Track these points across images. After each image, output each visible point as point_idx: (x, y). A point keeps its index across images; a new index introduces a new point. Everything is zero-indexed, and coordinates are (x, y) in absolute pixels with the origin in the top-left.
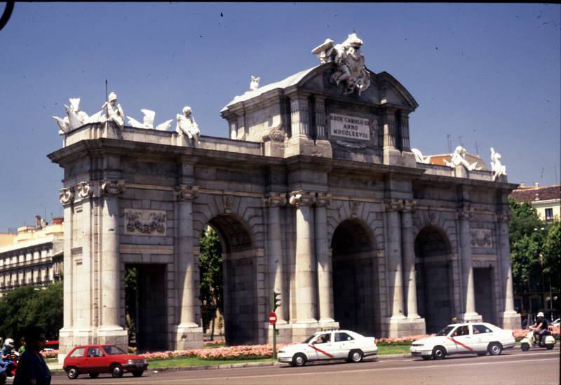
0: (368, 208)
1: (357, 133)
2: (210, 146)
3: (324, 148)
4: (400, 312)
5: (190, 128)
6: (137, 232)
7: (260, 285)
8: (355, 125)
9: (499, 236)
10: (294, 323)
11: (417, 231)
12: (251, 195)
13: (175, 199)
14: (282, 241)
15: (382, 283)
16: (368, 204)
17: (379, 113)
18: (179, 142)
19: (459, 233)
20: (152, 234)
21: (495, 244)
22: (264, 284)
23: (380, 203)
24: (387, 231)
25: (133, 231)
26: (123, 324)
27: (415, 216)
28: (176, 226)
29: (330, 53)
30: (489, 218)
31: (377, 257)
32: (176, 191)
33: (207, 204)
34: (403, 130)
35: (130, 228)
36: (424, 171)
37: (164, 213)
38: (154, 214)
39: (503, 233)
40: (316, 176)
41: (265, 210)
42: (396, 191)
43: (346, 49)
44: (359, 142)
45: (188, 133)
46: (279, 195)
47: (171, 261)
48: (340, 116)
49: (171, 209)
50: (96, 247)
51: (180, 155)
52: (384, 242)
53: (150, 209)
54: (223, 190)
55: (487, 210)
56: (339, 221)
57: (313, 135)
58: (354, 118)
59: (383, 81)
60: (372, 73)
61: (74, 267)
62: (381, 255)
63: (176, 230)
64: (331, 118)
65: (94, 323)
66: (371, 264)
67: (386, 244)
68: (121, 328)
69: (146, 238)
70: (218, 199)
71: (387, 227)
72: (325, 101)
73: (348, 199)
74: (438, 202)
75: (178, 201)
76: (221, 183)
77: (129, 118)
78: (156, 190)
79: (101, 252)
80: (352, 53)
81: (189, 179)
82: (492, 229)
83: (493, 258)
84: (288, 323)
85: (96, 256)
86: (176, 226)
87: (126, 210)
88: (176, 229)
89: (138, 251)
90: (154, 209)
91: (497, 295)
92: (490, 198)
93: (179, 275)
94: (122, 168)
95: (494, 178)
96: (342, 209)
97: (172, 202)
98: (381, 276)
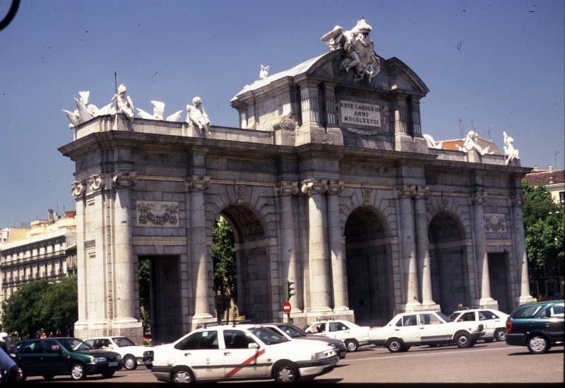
0: (381, 194)
1: (368, 120)
2: (220, 136)
3: (335, 136)
4: (415, 298)
5: (200, 117)
6: (149, 224)
7: (274, 274)
8: (365, 111)
9: (514, 220)
10: (308, 311)
11: (431, 218)
12: (263, 184)
13: (187, 190)
14: (295, 230)
15: (396, 270)
16: (379, 192)
17: (389, 99)
18: (190, 133)
19: (472, 218)
21: (509, 229)
22: (278, 274)
23: (392, 190)
24: (401, 218)
25: (145, 223)
26: (137, 316)
27: (428, 201)
28: (188, 217)
29: (339, 39)
30: (503, 202)
31: (390, 245)
32: (188, 182)
34: (414, 115)
36: (437, 156)
37: (176, 204)
38: (166, 206)
39: (517, 217)
40: (328, 163)
41: (277, 199)
42: (408, 177)
43: (355, 36)
44: (370, 129)
45: (198, 124)
46: (291, 184)
47: (183, 252)
48: (350, 103)
49: (183, 200)
50: (109, 239)
51: (191, 145)
52: (397, 229)
53: (162, 201)
54: (234, 181)
55: (500, 194)
56: (352, 208)
57: (323, 123)
58: (364, 105)
59: (393, 67)
61: (88, 260)
62: (394, 241)
63: (188, 221)
64: (342, 105)
65: (108, 315)
66: (385, 251)
67: (399, 231)
68: (136, 320)
70: (230, 189)
71: (400, 214)
72: (336, 88)
73: (359, 186)
74: (451, 187)
75: (190, 192)
76: (231, 172)
77: (139, 109)
78: (167, 181)
79: (114, 245)
80: (361, 40)
81: (199, 170)
82: (506, 214)
83: (508, 243)
84: (303, 312)
85: (109, 249)
86: (188, 217)
87: (138, 202)
88: (188, 220)
89: (151, 243)
90: (167, 201)
91: (512, 280)
92: (503, 182)
93: (192, 266)
94: (133, 160)
95: (507, 162)
96: (354, 198)
97: (184, 193)
98: (395, 263)
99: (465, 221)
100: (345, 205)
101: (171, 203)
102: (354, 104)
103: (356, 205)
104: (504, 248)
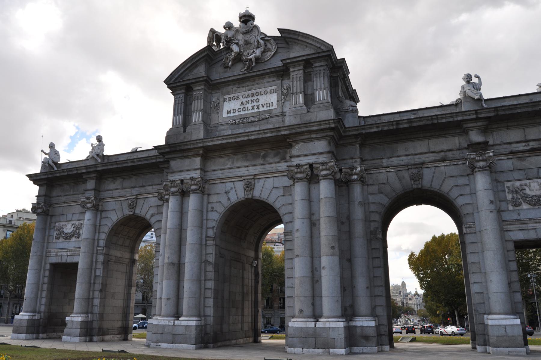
0: (270, 183)
6: (61, 240)
8: (256, 98)
19: (473, 193)
20: (71, 240)
35: (57, 238)
37: (81, 222)
40: (187, 162)
44: (260, 113)
48: (236, 95)
53: (72, 220)
54: (125, 196)
56: (227, 204)
58: (254, 91)
60: (274, 38)
64: (225, 100)
87: (57, 224)
99: (461, 197)
100: (220, 202)
101: (78, 221)
102: (241, 95)
103: (234, 199)
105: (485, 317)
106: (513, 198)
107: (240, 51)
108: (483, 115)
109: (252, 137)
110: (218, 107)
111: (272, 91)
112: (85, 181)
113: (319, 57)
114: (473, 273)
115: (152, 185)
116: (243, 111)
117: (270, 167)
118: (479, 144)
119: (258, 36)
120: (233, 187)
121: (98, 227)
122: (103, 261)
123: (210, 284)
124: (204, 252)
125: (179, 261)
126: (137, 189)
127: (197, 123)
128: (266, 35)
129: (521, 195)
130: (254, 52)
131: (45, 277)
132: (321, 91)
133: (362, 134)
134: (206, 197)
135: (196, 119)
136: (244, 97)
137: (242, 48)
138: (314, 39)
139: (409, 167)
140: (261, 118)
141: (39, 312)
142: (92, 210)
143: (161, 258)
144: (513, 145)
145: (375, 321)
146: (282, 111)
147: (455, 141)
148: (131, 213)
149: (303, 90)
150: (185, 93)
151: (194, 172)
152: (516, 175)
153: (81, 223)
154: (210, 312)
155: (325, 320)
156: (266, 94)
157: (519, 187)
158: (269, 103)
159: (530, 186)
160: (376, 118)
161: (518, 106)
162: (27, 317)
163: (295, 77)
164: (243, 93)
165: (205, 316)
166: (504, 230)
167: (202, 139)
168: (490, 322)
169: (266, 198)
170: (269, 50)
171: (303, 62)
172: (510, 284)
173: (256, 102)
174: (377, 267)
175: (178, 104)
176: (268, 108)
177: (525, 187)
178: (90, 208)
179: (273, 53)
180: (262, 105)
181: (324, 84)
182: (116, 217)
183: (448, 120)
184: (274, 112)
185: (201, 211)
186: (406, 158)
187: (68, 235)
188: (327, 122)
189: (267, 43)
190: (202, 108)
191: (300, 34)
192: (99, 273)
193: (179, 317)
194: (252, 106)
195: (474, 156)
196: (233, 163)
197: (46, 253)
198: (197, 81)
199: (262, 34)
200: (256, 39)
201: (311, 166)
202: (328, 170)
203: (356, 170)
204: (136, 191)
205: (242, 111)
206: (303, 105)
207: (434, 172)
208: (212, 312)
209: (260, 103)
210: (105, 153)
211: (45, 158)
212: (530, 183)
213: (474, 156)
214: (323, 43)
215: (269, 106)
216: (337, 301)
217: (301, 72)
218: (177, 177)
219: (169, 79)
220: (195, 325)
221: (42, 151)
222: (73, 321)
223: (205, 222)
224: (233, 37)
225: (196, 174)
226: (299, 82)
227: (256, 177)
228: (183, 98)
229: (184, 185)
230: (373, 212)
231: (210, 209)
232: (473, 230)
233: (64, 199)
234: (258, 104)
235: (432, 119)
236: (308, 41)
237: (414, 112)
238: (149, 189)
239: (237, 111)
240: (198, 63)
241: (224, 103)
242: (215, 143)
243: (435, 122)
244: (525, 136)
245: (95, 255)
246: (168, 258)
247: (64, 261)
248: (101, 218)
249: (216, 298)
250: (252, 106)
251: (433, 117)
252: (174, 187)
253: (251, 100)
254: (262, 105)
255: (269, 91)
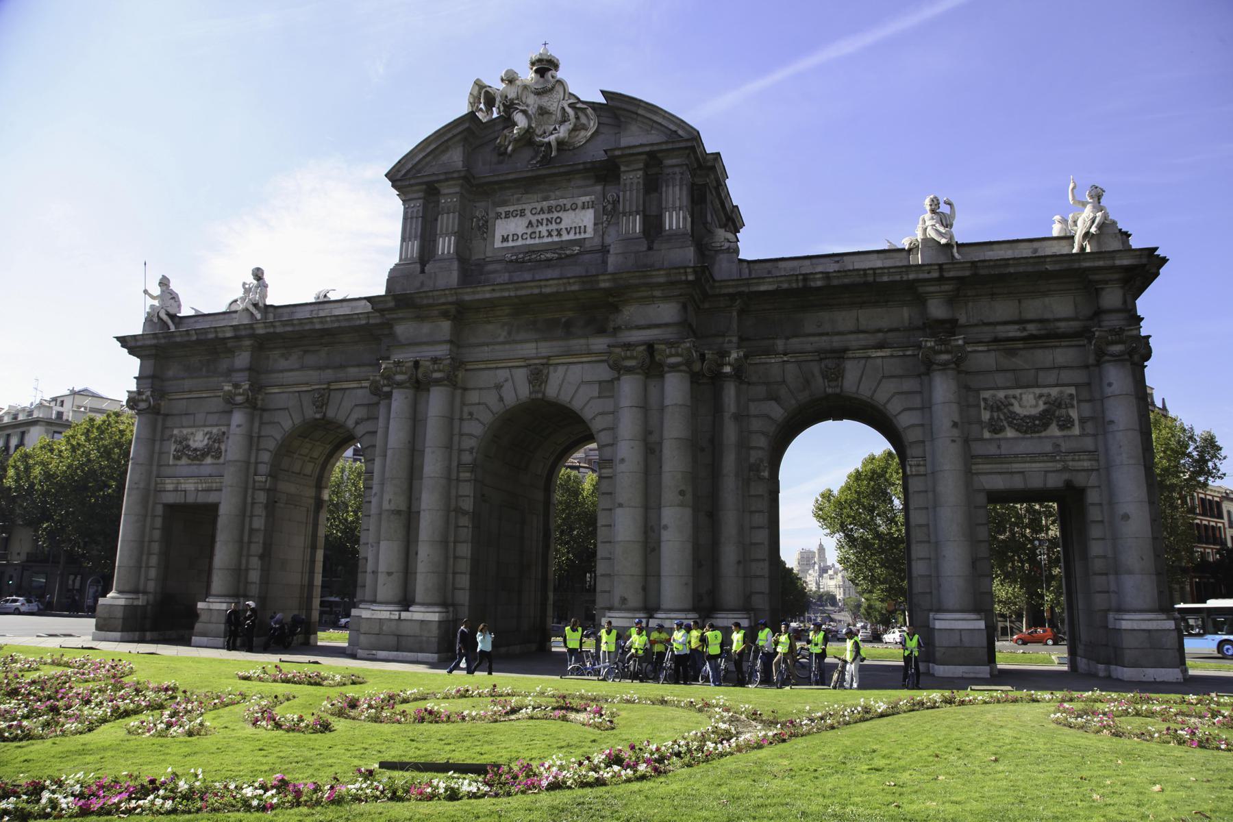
0: (576, 373)
6: (184, 461)
8: (555, 215)
19: (927, 407)
20: (204, 463)
21: (1090, 428)
33: (287, 409)
35: (177, 458)
37: (224, 429)
40: (426, 328)
48: (519, 207)
53: (205, 426)
56: (497, 408)
58: (553, 203)
60: (593, 105)
64: (498, 216)
69: (195, 467)
82: (1076, 386)
87: (176, 432)
91: (1098, 565)
96: (508, 386)
100: (482, 404)
102: (528, 207)
103: (510, 399)
104: (1066, 476)
105: (931, 615)
106: (992, 418)
107: (530, 127)
108: (952, 274)
109: (547, 290)
110: (485, 228)
111: (586, 204)
112: (231, 352)
113: (673, 149)
114: (918, 542)
115: (358, 366)
116: (531, 238)
117: (577, 344)
118: (941, 322)
119: (563, 99)
120: (509, 377)
121: (256, 439)
122: (265, 502)
123: (465, 550)
124: (453, 492)
125: (409, 508)
126: (329, 371)
127: (447, 257)
128: (578, 99)
129: (1004, 414)
130: (555, 129)
131: (154, 529)
132: (674, 213)
133: (741, 294)
134: (459, 392)
135: (443, 250)
136: (533, 212)
137: (534, 121)
138: (666, 115)
139: (822, 356)
140: (563, 254)
141: (145, 593)
142: (246, 407)
143: (374, 500)
144: (999, 328)
145: (749, 618)
146: (603, 243)
147: (904, 314)
148: (318, 416)
149: (641, 208)
150: (424, 198)
151: (438, 347)
152: (1000, 379)
153: (223, 430)
154: (463, 597)
155: (663, 616)
156: (575, 210)
157: (1003, 400)
158: (580, 227)
159: (1021, 399)
160: (768, 265)
161: (1011, 262)
162: (122, 602)
163: (628, 181)
164: (532, 203)
165: (453, 605)
166: (973, 471)
167: (455, 289)
168: (938, 625)
169: (568, 399)
170: (585, 128)
171: (644, 157)
172: (974, 562)
173: (556, 223)
174: (759, 528)
175: (412, 218)
176: (578, 237)
177: (1013, 401)
178: (241, 404)
179: (590, 134)
180: (566, 229)
181: (679, 199)
182: (290, 422)
183: (891, 278)
184: (588, 245)
185: (451, 420)
186: (817, 339)
187: (198, 453)
188: (682, 271)
189: (580, 114)
190: (456, 229)
191: (641, 104)
192: (259, 523)
193: (409, 606)
194: (548, 231)
195: (933, 344)
196: (509, 333)
197: (157, 484)
198: (448, 177)
199: (572, 97)
200: (560, 105)
201: (650, 347)
202: (681, 355)
203: (729, 357)
204: (329, 374)
205: (529, 238)
206: (641, 235)
207: (865, 365)
208: (467, 598)
209: (563, 226)
210: (268, 302)
211: (152, 307)
212: (1021, 394)
213: (933, 344)
214: (682, 124)
215: (580, 233)
216: (686, 584)
217: (640, 173)
218: (405, 356)
219: (394, 170)
220: (437, 619)
221: (146, 292)
222: (211, 610)
223: (456, 438)
224: (517, 99)
225: (442, 350)
226: (635, 192)
227: (551, 362)
228: (421, 208)
229: (421, 370)
230: (756, 432)
231: (465, 416)
232: (922, 469)
233: (188, 384)
234: (559, 227)
235: (865, 275)
236: (655, 118)
237: (837, 259)
238: (353, 371)
239: (520, 239)
240: (450, 143)
241: (497, 221)
242: (477, 297)
243: (871, 279)
244: (1020, 312)
245: (250, 492)
246: (390, 501)
247: (191, 499)
248: (262, 423)
249: (474, 573)
250: (548, 231)
251: (868, 272)
252: (401, 373)
253: (547, 219)
254: (566, 229)
255: (580, 204)
